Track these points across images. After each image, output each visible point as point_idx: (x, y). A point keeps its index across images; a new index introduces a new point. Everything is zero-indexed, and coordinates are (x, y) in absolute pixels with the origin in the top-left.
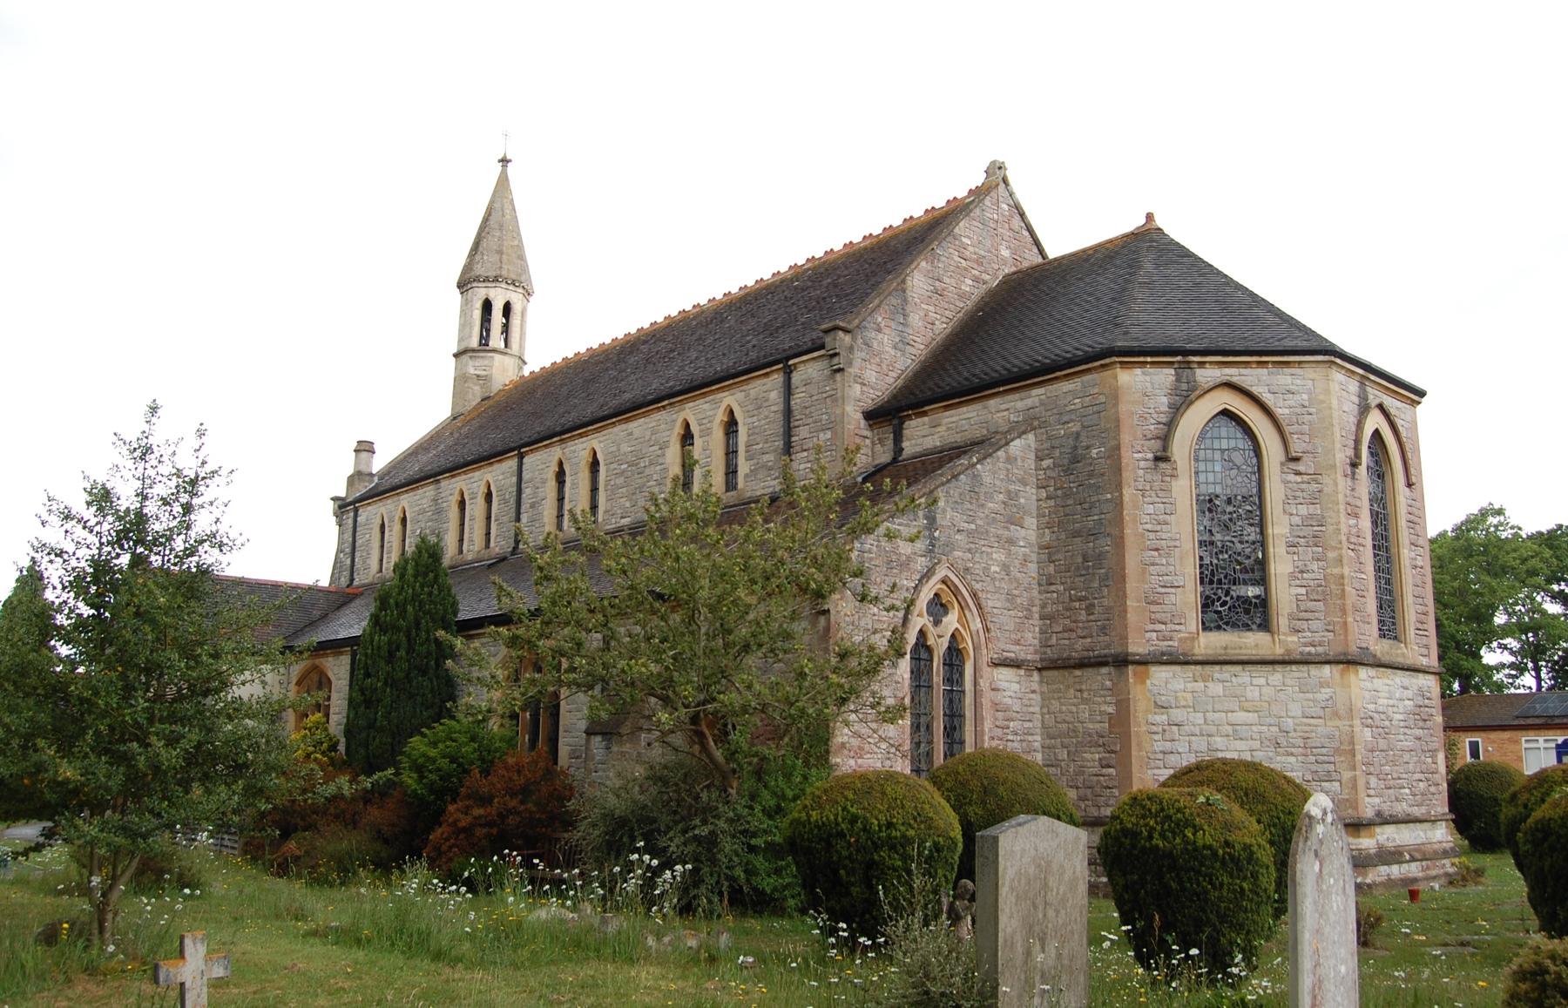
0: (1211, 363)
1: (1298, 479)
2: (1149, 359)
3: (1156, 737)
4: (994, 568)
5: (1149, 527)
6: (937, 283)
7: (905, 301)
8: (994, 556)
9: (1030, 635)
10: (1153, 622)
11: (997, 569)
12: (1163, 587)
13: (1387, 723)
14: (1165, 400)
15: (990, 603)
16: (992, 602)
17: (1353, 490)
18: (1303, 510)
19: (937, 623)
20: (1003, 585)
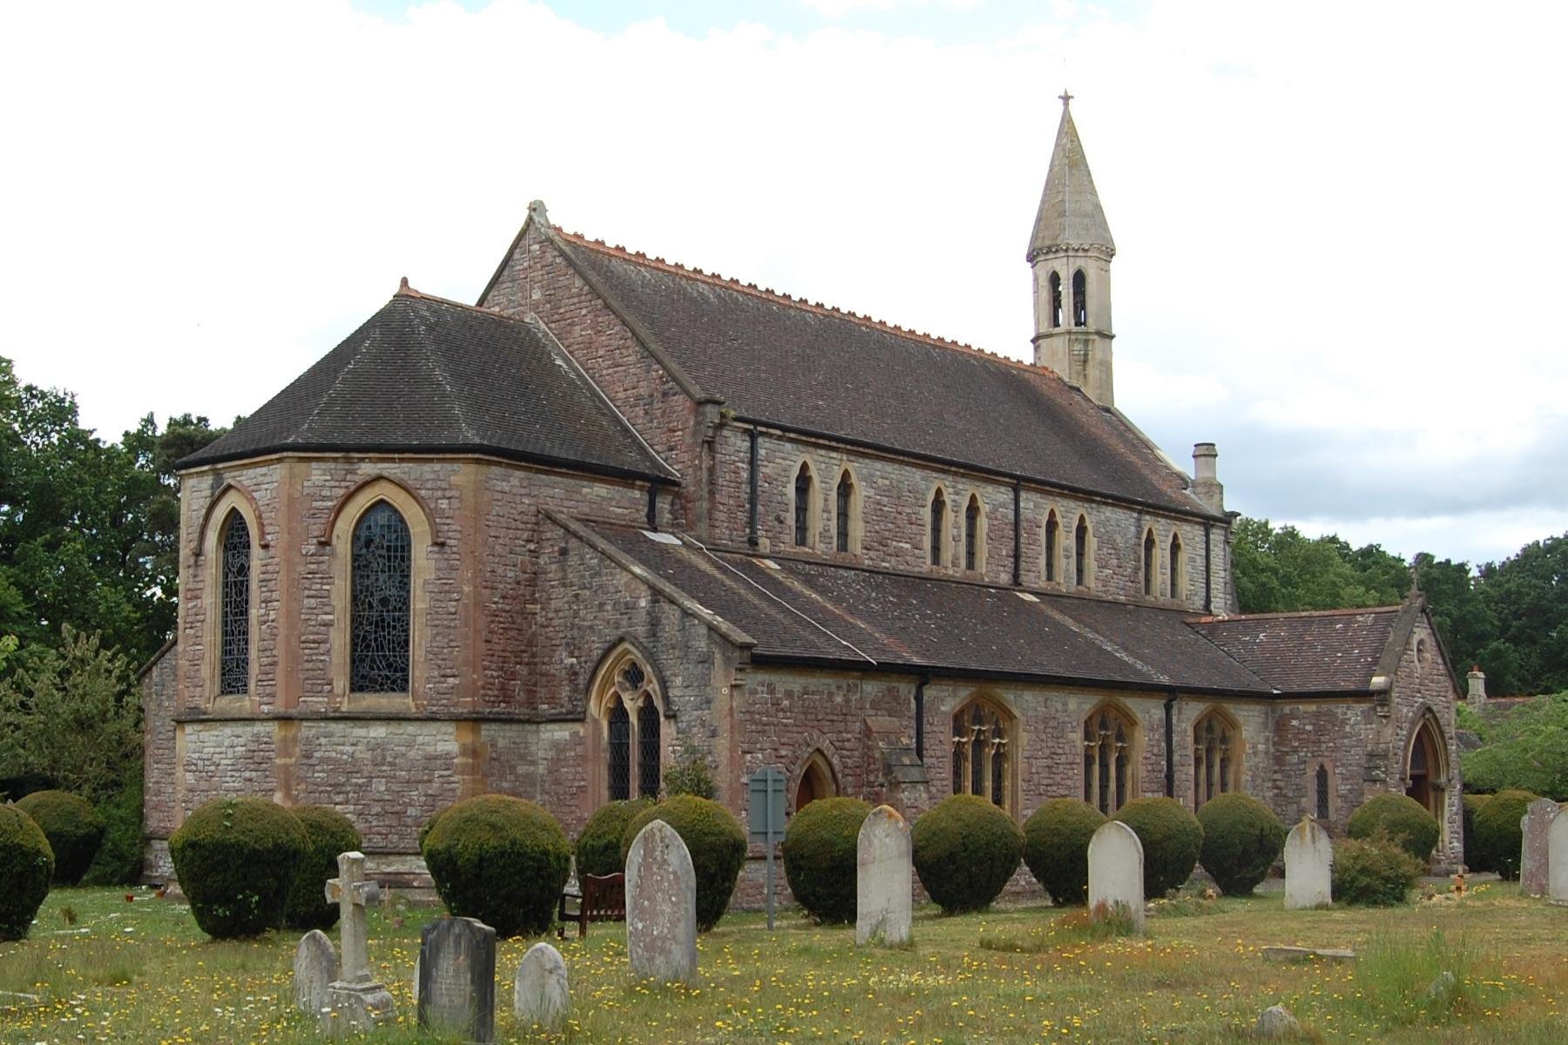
13: (212, 768)
17: (195, 576)
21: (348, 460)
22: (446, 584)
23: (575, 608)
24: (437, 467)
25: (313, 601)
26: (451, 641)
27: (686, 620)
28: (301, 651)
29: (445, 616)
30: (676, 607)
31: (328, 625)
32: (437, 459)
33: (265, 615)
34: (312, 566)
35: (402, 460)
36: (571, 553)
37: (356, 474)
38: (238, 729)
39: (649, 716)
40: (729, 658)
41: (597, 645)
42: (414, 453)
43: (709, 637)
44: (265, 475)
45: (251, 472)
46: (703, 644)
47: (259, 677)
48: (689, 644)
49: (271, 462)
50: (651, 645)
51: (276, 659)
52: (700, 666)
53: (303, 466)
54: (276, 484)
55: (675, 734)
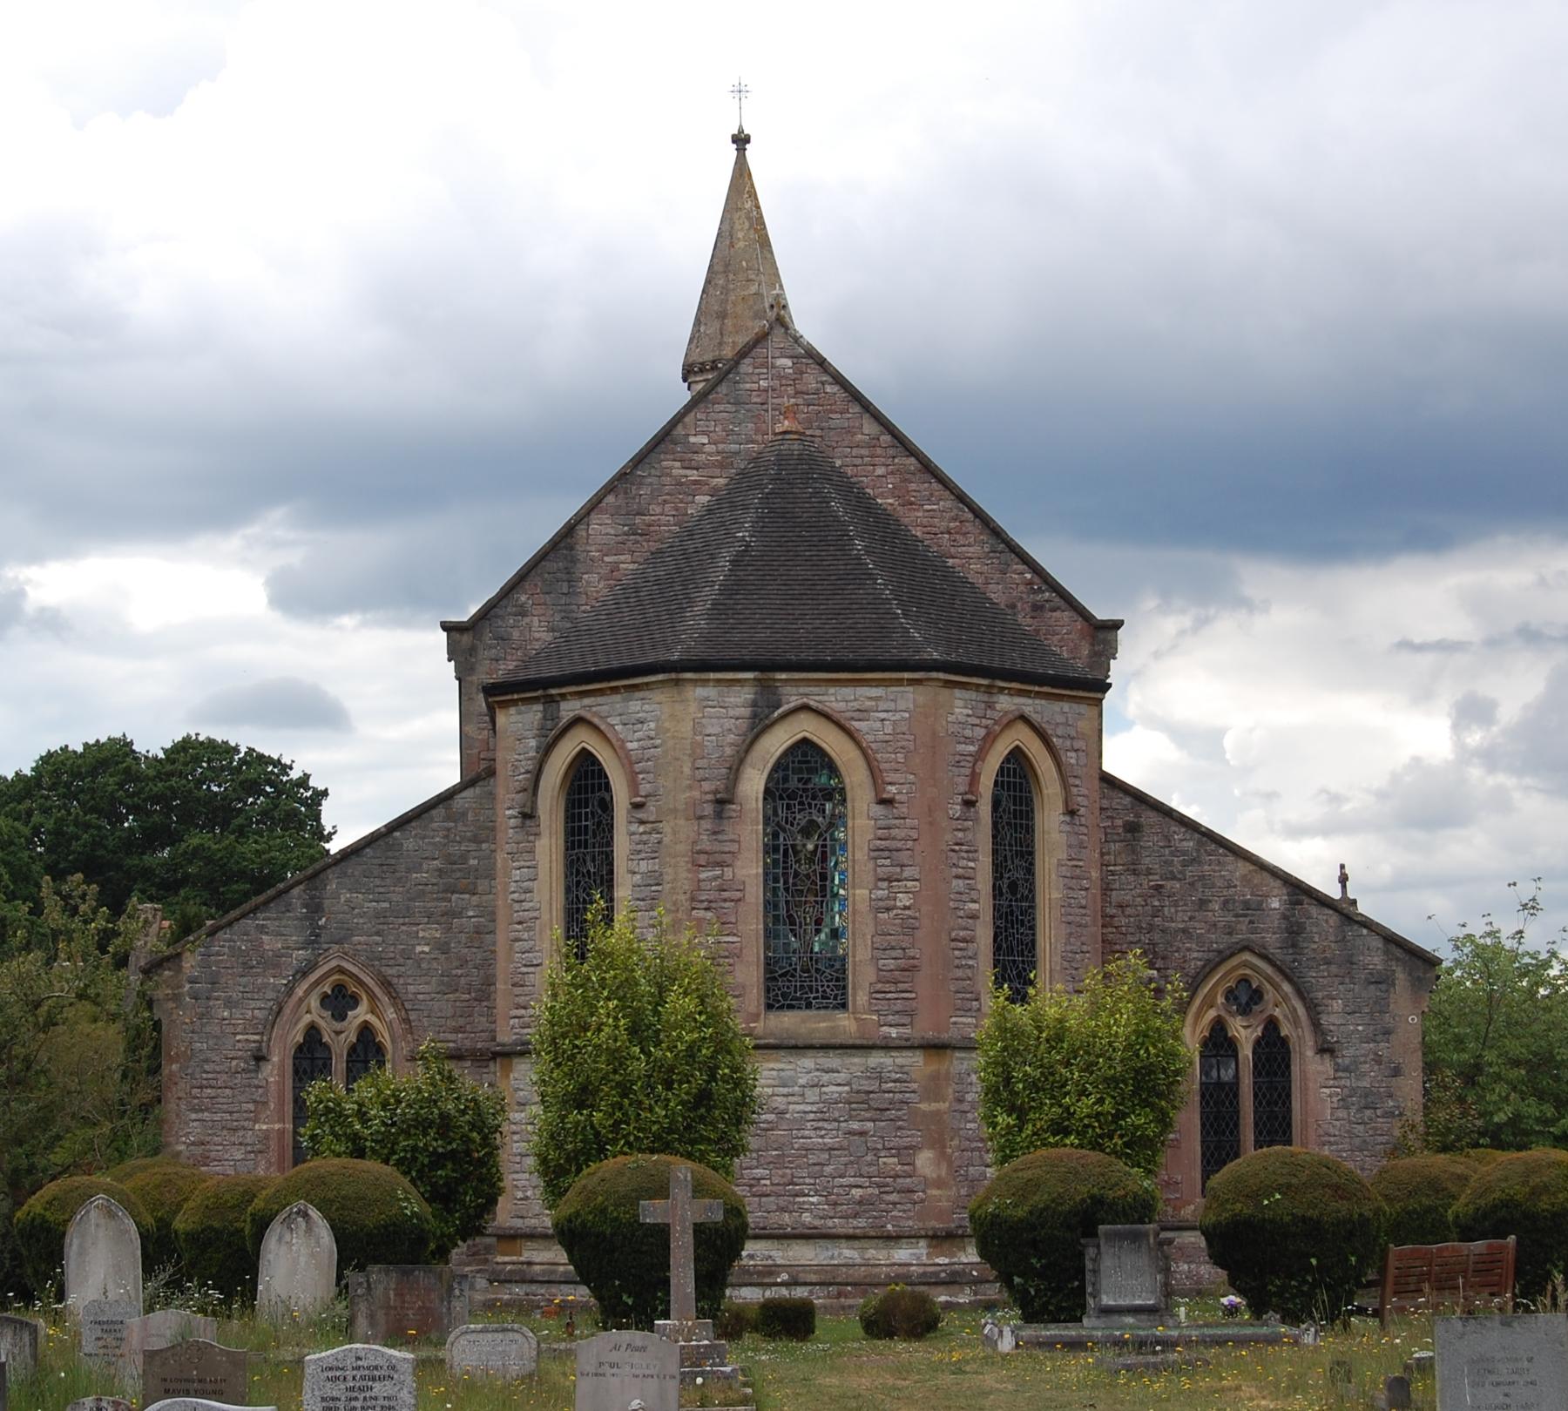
0: (570, 693)
1: (641, 829)
2: (516, 697)
3: (516, 1137)
4: (419, 949)
5: (515, 896)
6: (638, 520)
7: (574, 561)
8: (421, 934)
9: (484, 1019)
10: (518, 1007)
11: (426, 949)
12: (525, 966)
14: (533, 743)
15: (411, 988)
16: (414, 988)
18: (644, 866)
19: (340, 1016)
20: (435, 965)
21: (989, 690)
22: (1076, 866)
23: (1157, 903)
24: (1066, 706)
25: (960, 882)
26: (1083, 944)
27: (1347, 928)
28: (951, 952)
29: (1077, 910)
30: (1331, 912)
31: (974, 917)
32: (1069, 696)
33: (888, 898)
34: (960, 835)
35: (1038, 695)
36: (1147, 830)
37: (994, 709)
38: (832, 1060)
39: (1274, 1050)
40: (1419, 979)
41: (1195, 955)
42: (1053, 687)
43: (1386, 952)
44: (877, 699)
45: (847, 692)
46: (1376, 960)
47: (879, 986)
48: (1355, 959)
49: (899, 682)
50: (1290, 958)
51: (915, 962)
52: (1372, 987)
53: (946, 692)
54: (907, 715)
55: (1332, 1072)
